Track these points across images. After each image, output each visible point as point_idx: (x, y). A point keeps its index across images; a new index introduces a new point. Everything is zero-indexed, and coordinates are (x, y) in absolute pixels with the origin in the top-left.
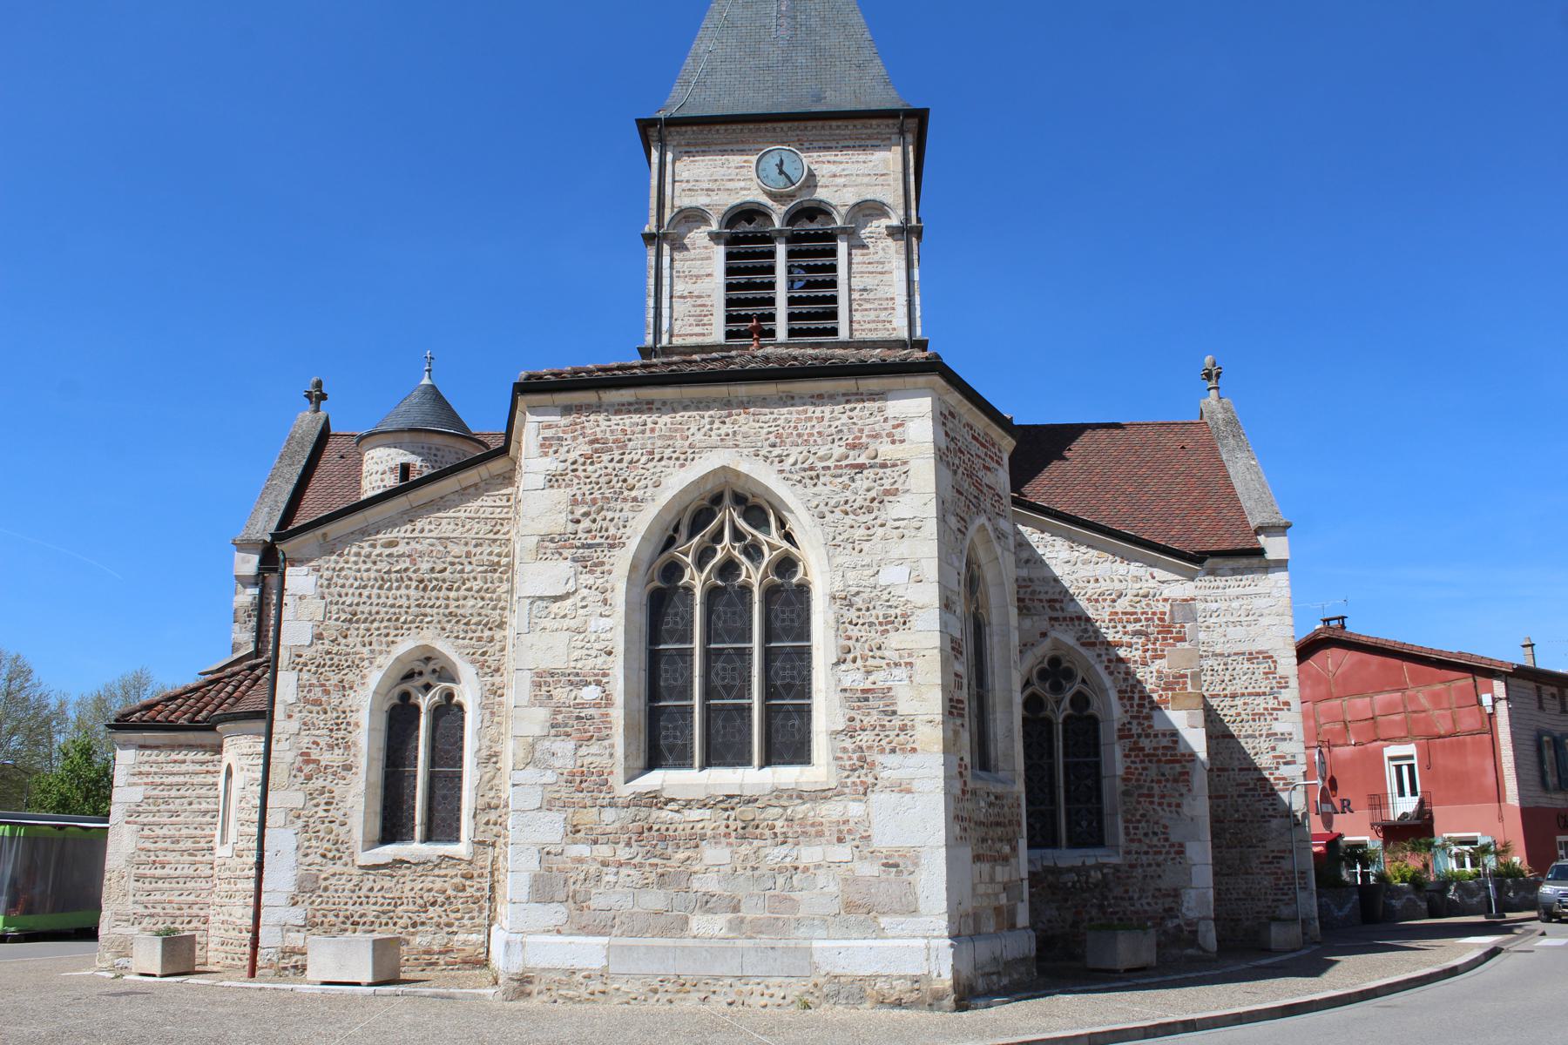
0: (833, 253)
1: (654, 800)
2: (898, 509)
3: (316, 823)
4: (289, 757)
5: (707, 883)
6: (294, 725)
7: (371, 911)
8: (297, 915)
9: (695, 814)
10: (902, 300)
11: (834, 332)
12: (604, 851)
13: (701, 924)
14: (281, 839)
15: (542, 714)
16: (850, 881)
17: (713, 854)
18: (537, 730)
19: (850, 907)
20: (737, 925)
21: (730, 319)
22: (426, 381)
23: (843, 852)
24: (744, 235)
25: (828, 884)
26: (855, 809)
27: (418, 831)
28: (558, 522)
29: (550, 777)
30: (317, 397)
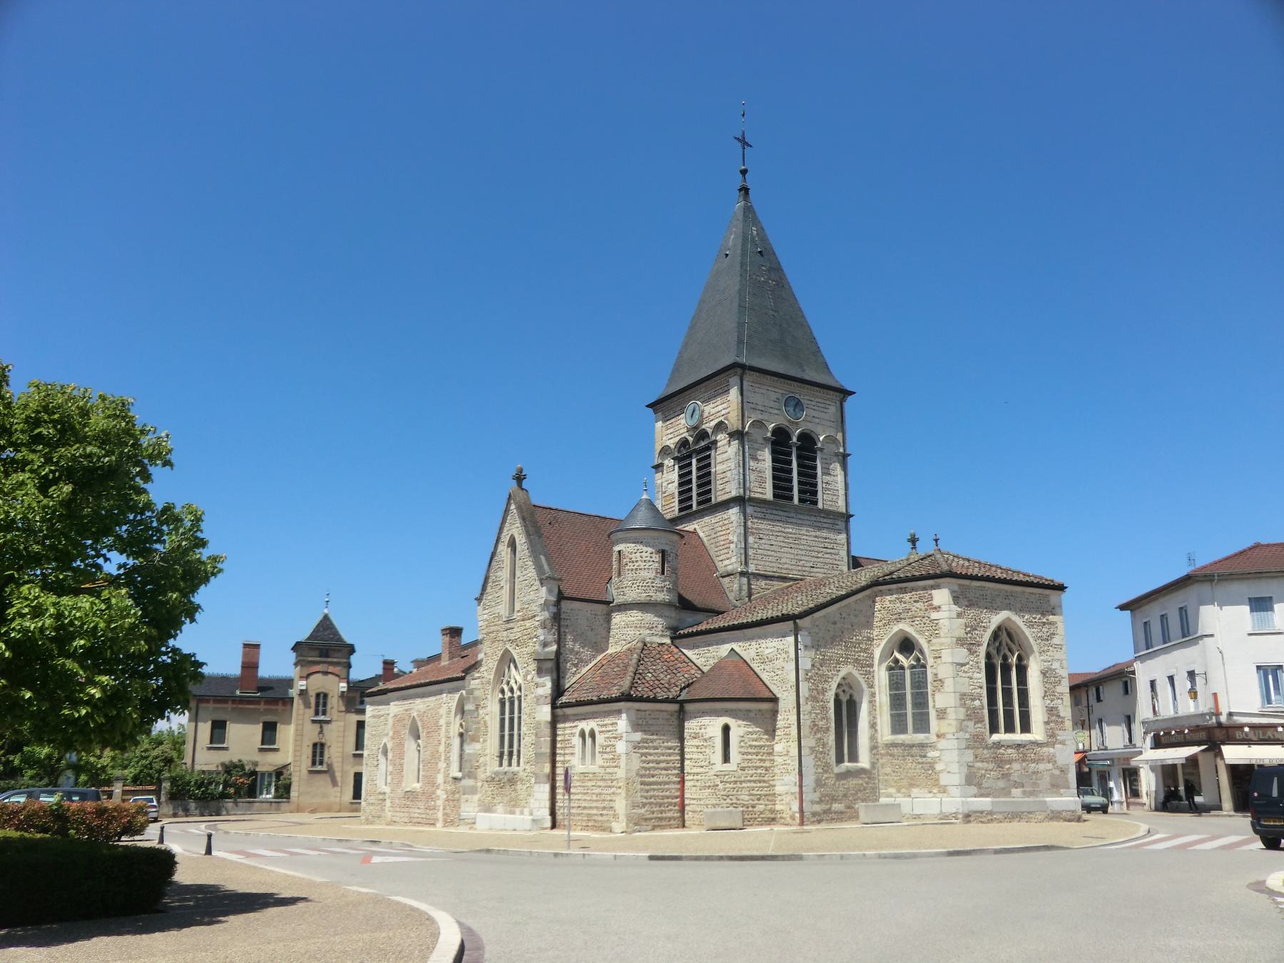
0: (815, 460)
1: (998, 745)
2: (1056, 640)
3: (818, 754)
4: (808, 722)
5: (1015, 777)
6: (808, 707)
7: (841, 794)
8: (816, 796)
9: (1010, 751)
10: (842, 492)
11: (816, 503)
12: (985, 765)
13: (1014, 791)
14: (808, 761)
15: (963, 710)
16: (1052, 776)
17: (1016, 766)
18: (962, 717)
19: (1053, 786)
20: (1024, 793)
21: (775, 487)
22: (645, 497)
23: (1050, 766)
24: (780, 441)
25: (1047, 779)
26: (1051, 750)
27: (846, 757)
28: (961, 633)
29: (967, 736)
30: (519, 478)
